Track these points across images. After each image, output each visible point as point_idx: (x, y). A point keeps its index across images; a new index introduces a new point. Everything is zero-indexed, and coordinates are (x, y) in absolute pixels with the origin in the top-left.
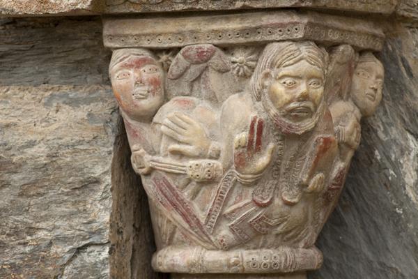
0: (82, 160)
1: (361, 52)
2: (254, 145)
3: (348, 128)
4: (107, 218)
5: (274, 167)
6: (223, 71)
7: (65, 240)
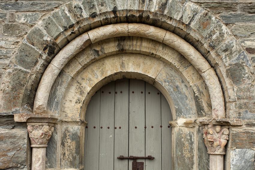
0: (24, 136)
1: (52, 126)
2: (42, 135)
3: (51, 134)
4: (26, 142)
5: (44, 137)
6: (39, 128)
7: (22, 144)
